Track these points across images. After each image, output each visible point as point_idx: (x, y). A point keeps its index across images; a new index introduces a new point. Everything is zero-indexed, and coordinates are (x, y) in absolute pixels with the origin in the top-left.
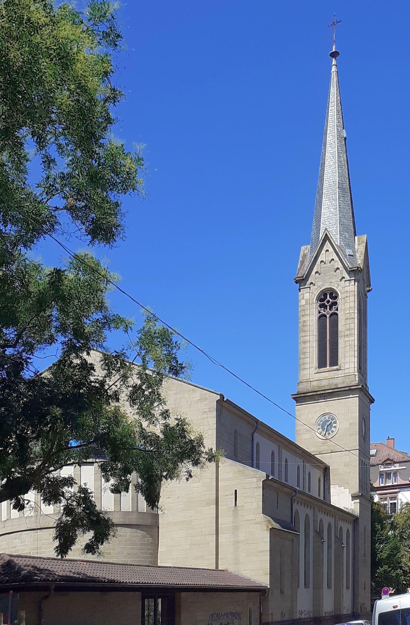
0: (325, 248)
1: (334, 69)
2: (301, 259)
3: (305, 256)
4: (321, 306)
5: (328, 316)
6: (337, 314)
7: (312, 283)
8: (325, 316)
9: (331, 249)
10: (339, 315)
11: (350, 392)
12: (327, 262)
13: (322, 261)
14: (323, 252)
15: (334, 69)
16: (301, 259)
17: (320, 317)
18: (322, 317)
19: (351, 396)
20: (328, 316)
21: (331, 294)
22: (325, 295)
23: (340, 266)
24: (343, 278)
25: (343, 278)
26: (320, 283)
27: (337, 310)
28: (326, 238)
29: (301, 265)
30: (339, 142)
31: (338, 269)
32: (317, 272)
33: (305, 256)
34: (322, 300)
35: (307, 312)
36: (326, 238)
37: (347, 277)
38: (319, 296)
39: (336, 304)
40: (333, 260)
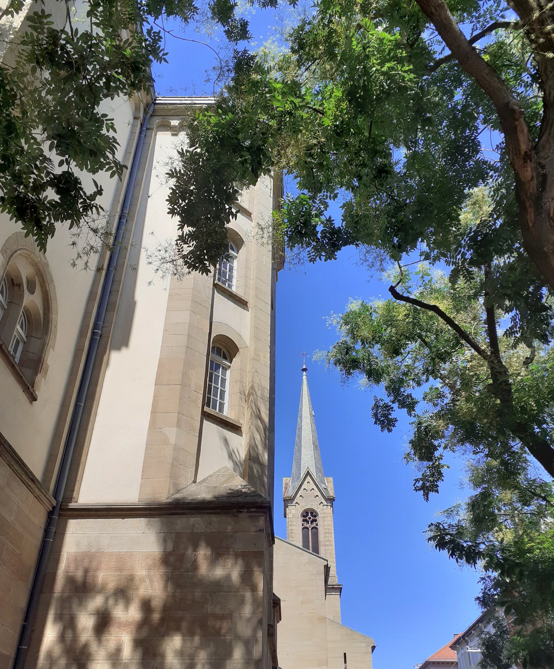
0: (307, 480)
1: (304, 377)
2: (284, 486)
3: (287, 484)
4: (304, 521)
5: (310, 528)
6: (317, 529)
7: (297, 503)
8: (308, 528)
9: (311, 482)
10: (319, 529)
11: (332, 590)
12: (309, 490)
13: (305, 489)
14: (306, 482)
15: (304, 377)
16: (284, 486)
17: (303, 529)
18: (305, 529)
19: (333, 593)
20: (310, 528)
21: (312, 513)
22: (307, 513)
23: (319, 494)
24: (322, 503)
25: (322, 503)
26: (304, 504)
27: (317, 525)
28: (308, 474)
29: (286, 490)
30: (311, 417)
31: (317, 496)
32: (301, 496)
33: (287, 484)
34: (304, 516)
35: (294, 523)
36: (308, 474)
37: (325, 503)
38: (302, 513)
39: (316, 521)
40: (313, 489)
